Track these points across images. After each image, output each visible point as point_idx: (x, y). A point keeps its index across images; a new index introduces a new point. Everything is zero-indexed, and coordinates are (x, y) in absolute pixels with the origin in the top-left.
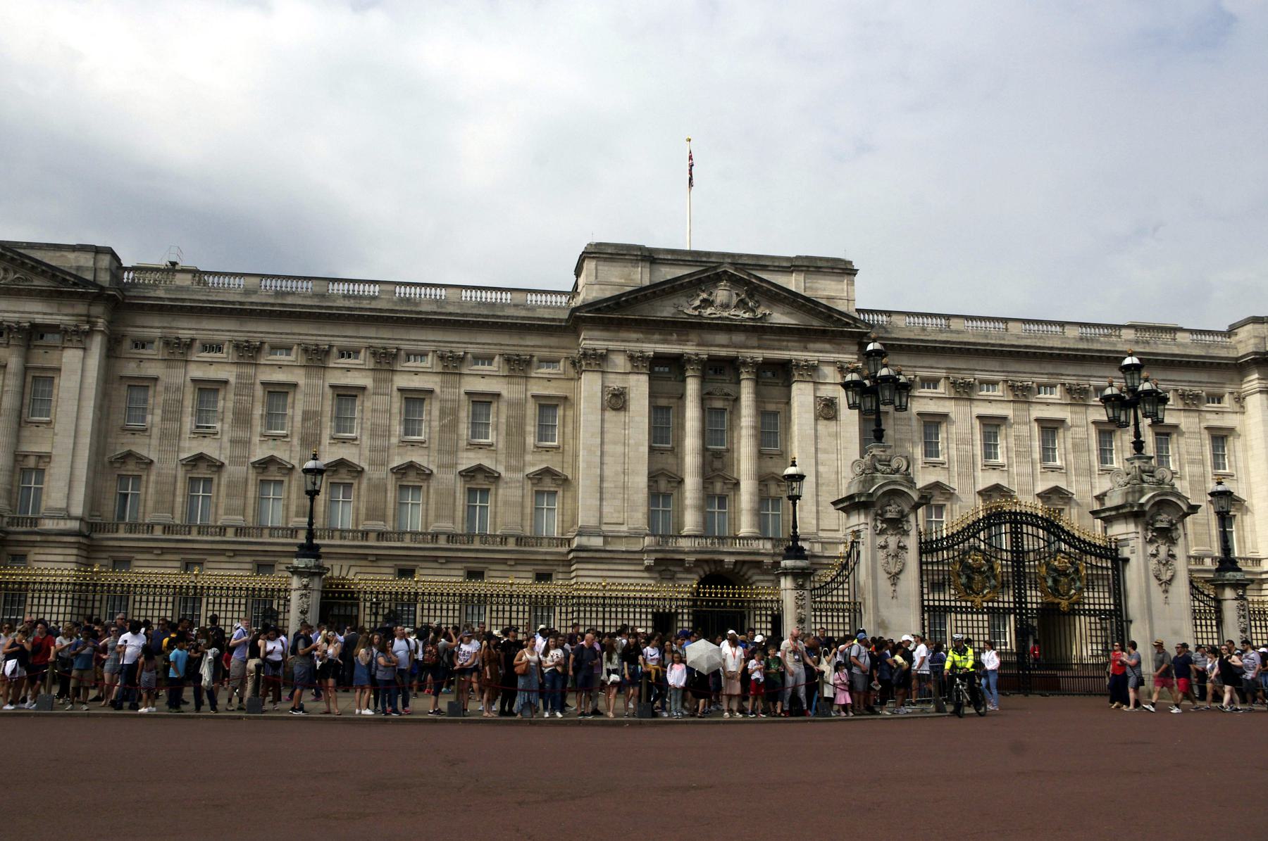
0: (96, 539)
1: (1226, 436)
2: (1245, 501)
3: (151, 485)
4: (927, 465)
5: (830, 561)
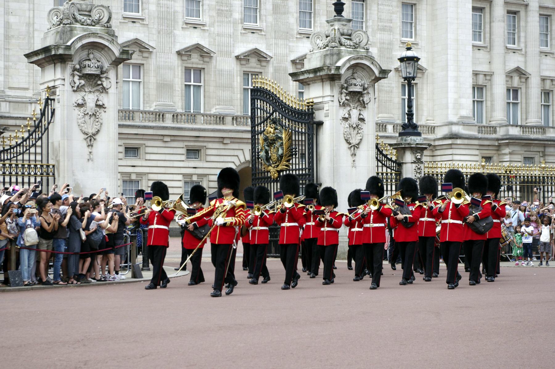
1: (415, 4)
2: (426, 70)
4: (126, 21)
5: (18, 122)
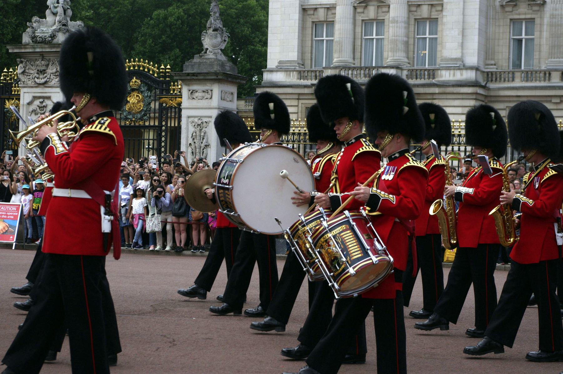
0: (495, 90)
3: (545, 27)
